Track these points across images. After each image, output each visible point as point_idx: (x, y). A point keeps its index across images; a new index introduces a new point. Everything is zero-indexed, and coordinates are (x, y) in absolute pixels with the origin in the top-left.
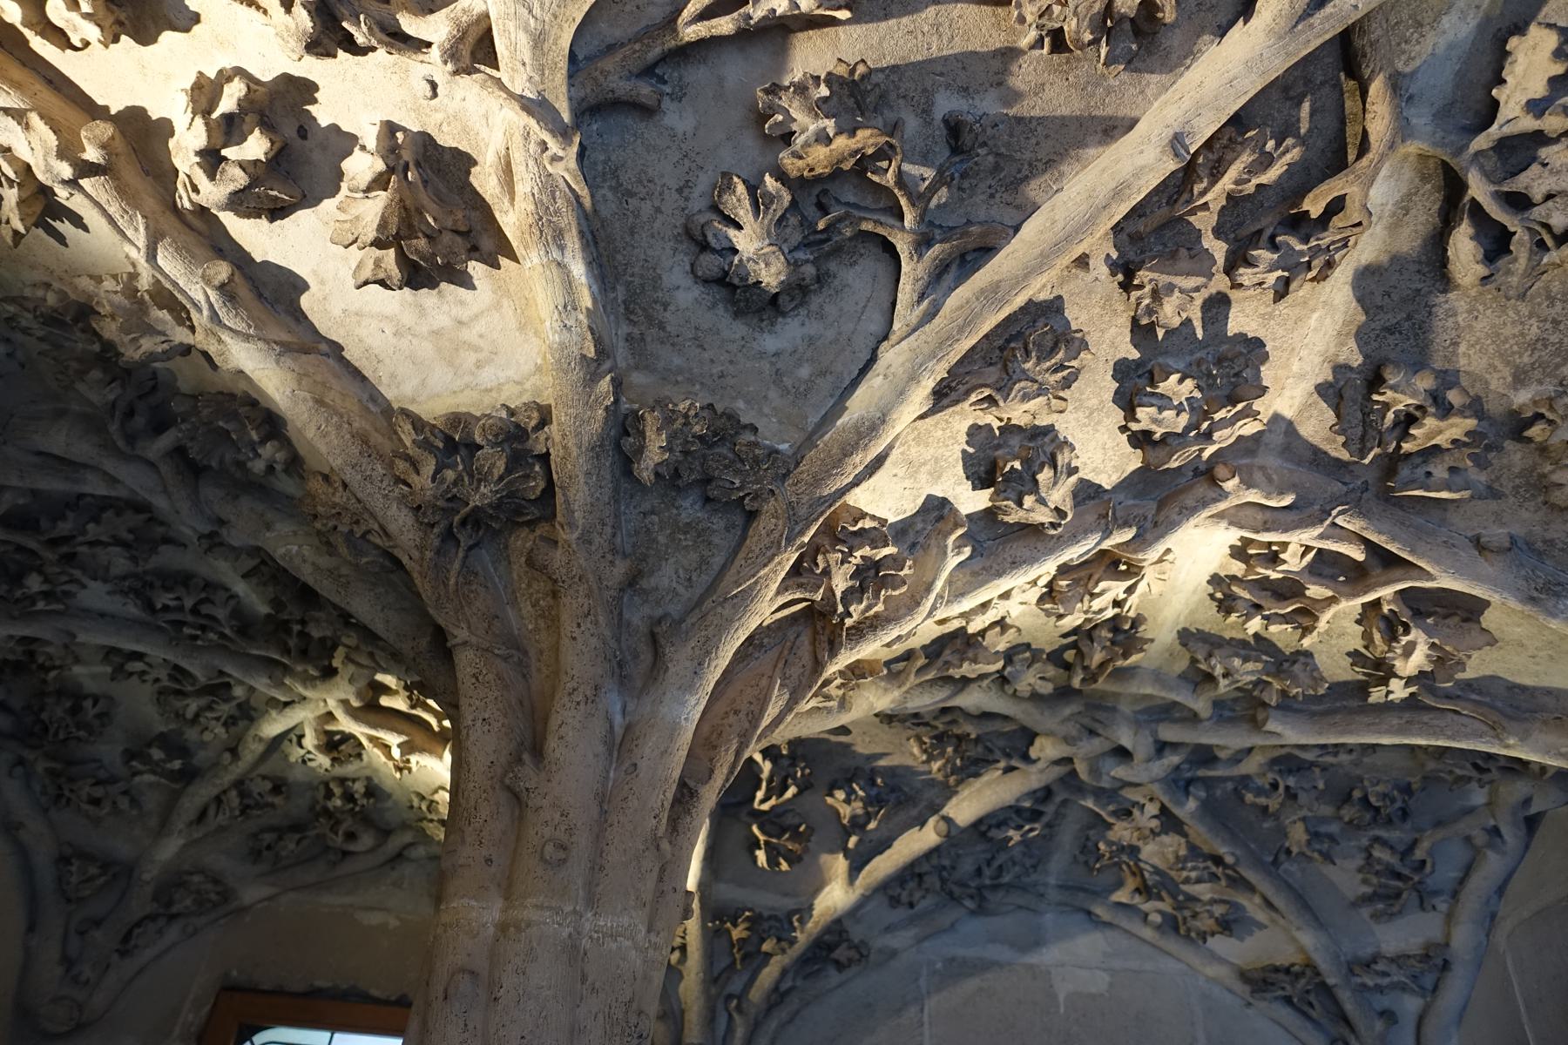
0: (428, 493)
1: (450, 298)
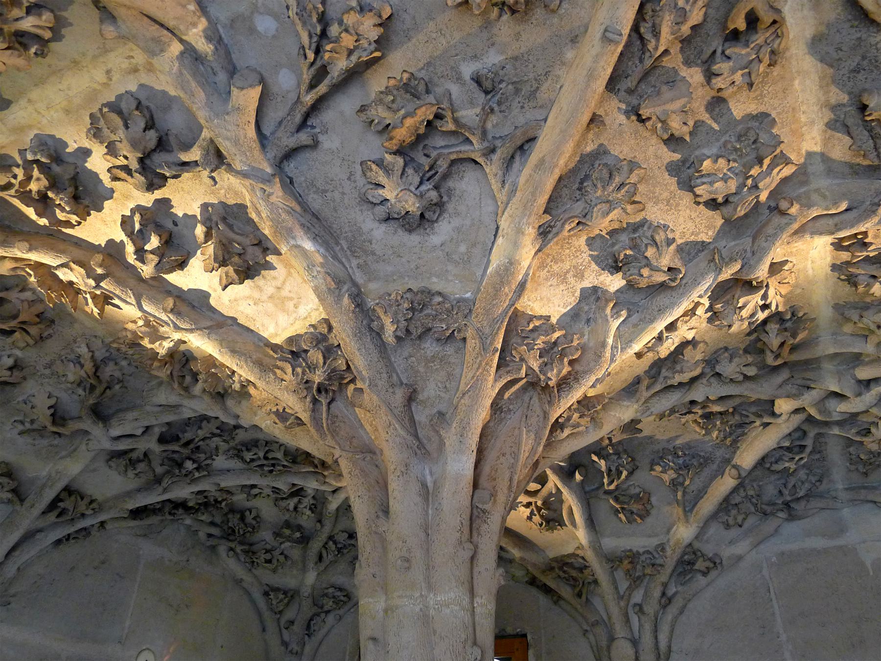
0: (294, 382)
1: (268, 278)
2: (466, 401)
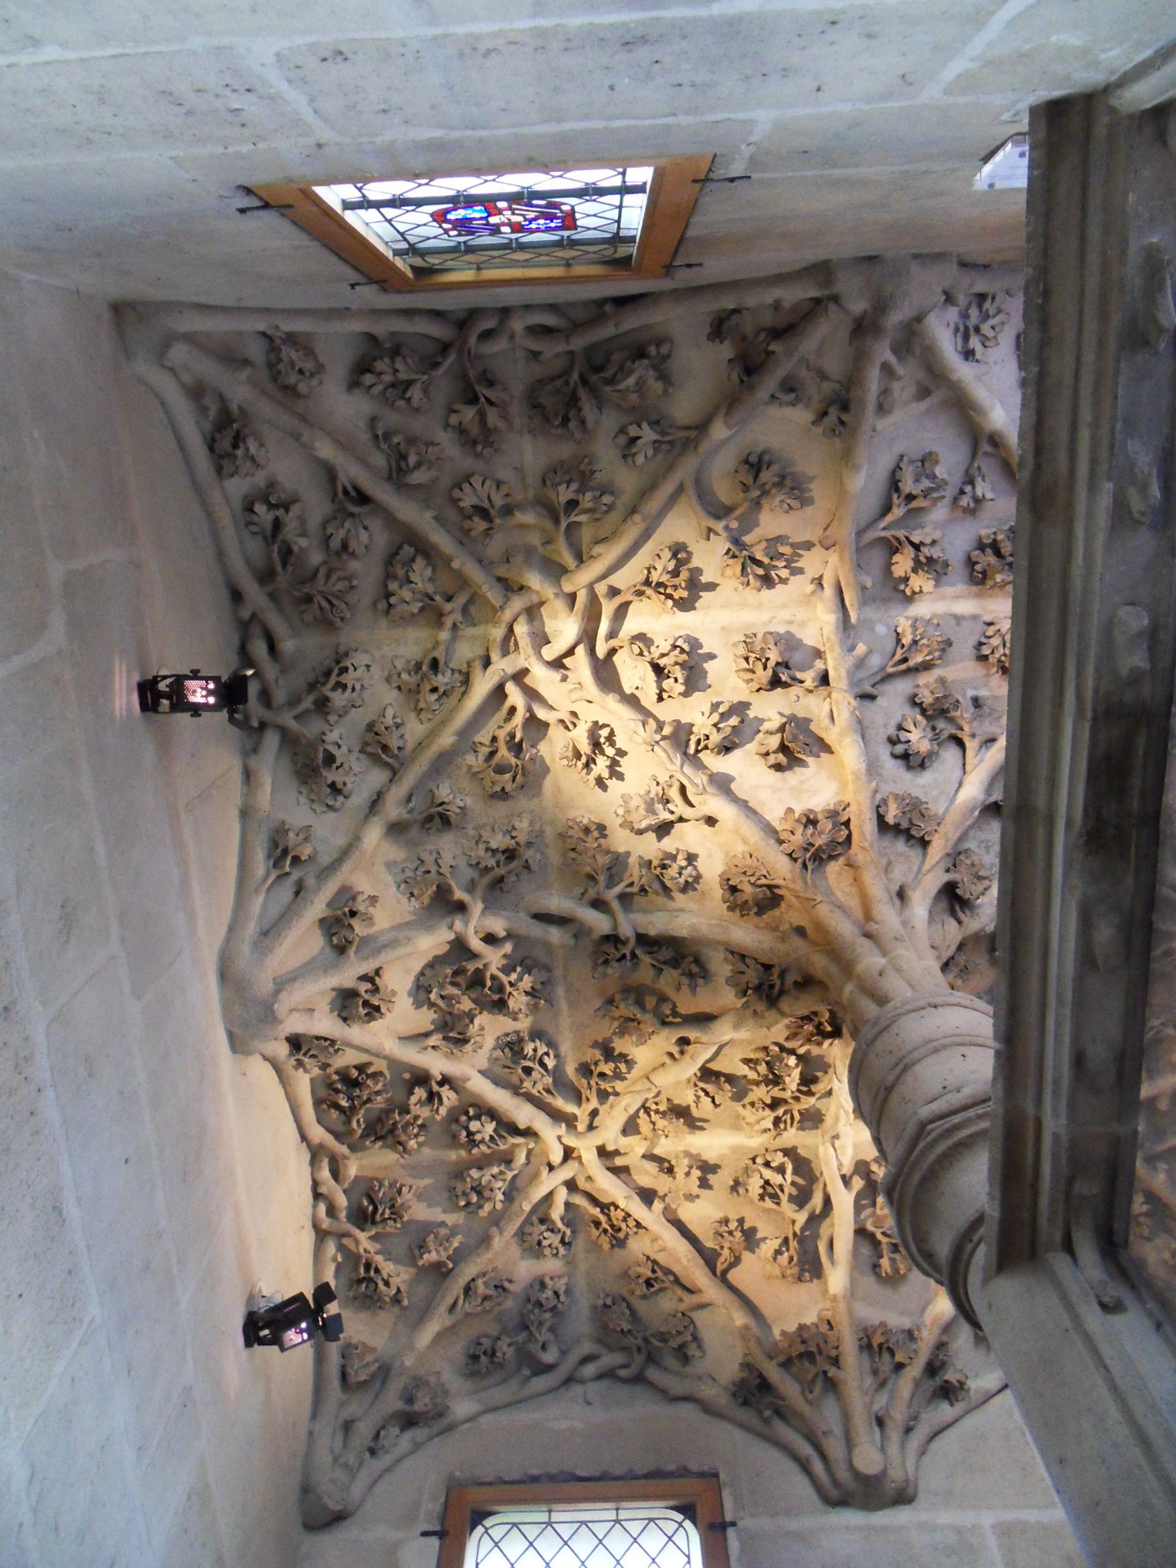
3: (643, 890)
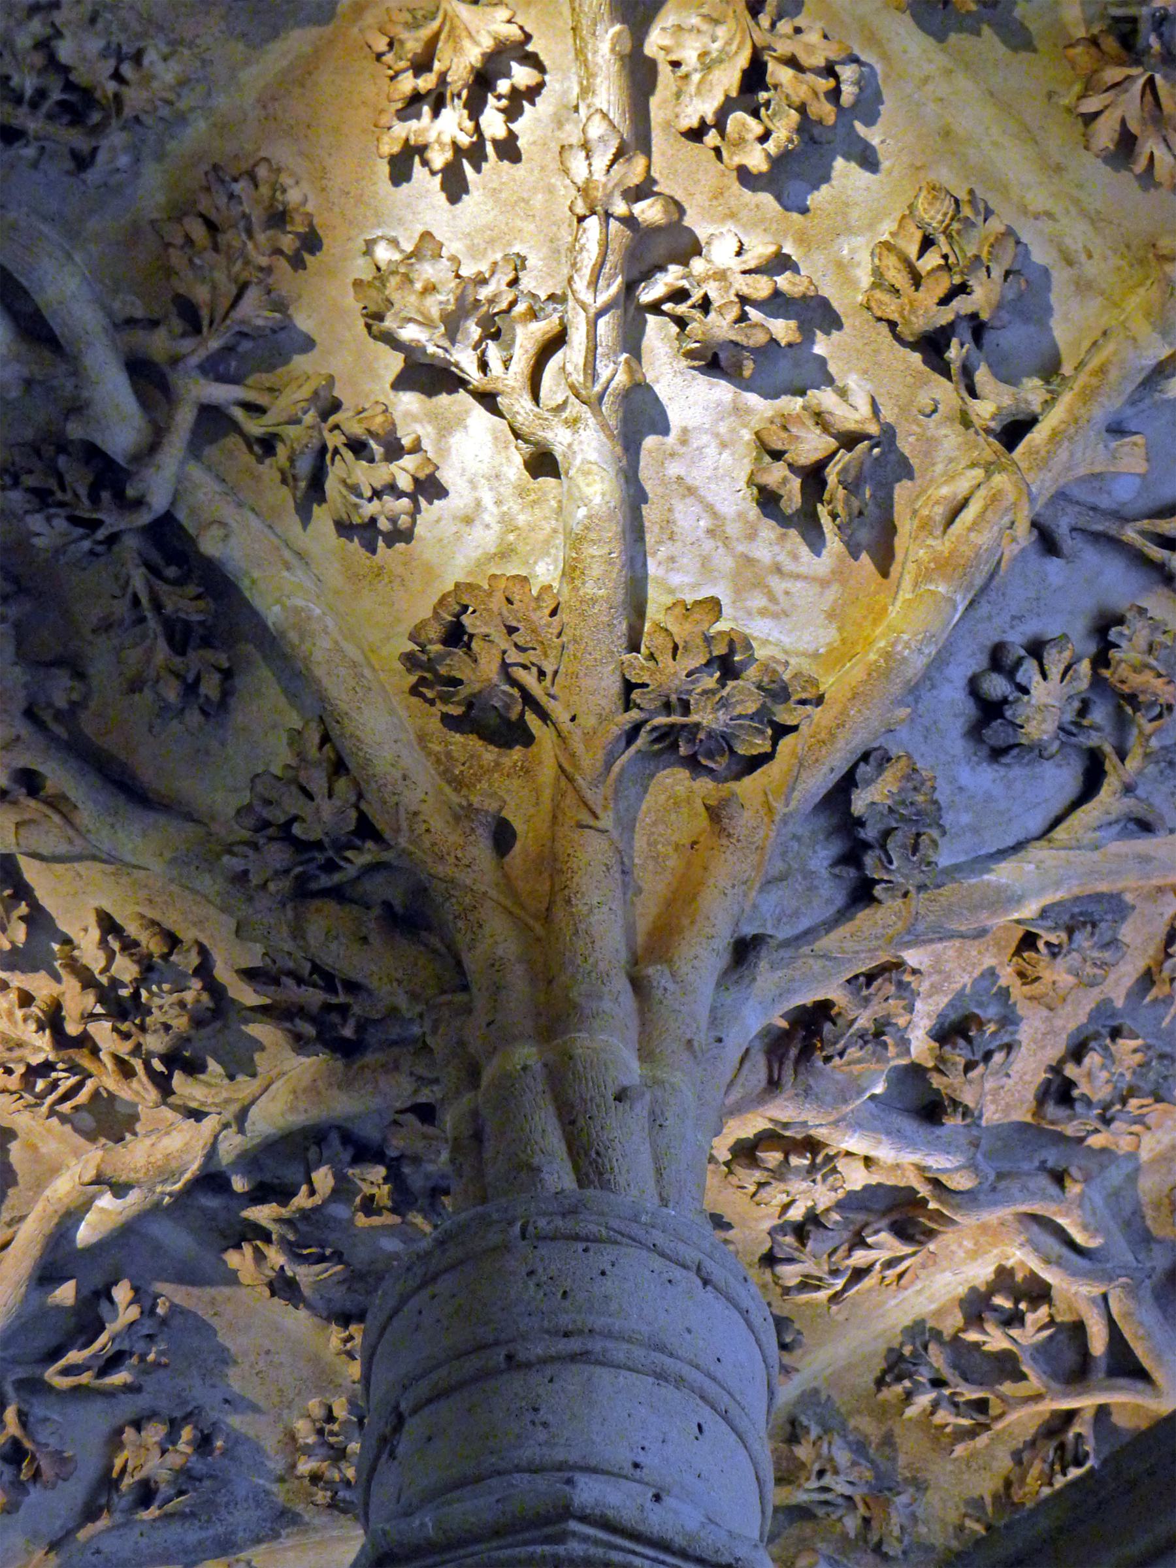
0: (677, 682)
1: (788, 546)
2: (817, 965)
3: (267, 445)
